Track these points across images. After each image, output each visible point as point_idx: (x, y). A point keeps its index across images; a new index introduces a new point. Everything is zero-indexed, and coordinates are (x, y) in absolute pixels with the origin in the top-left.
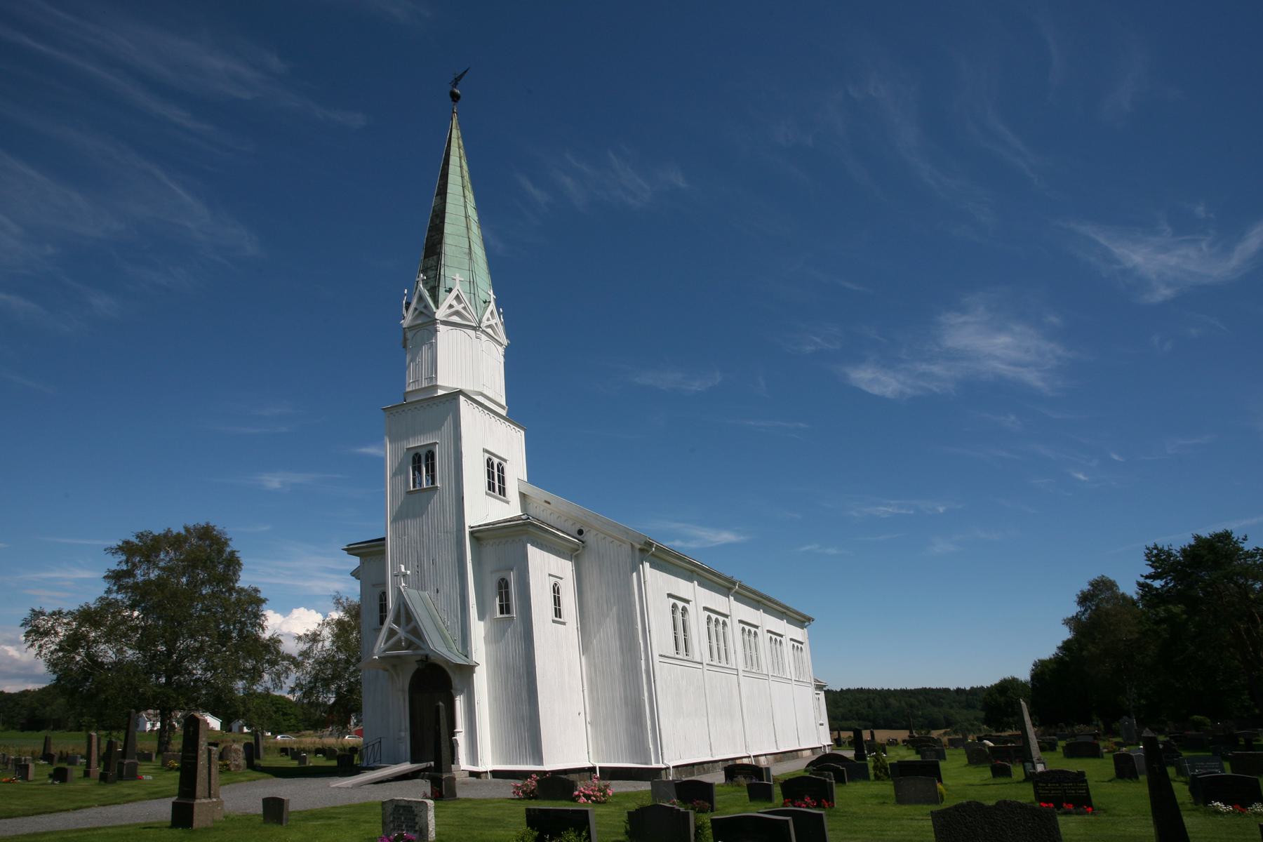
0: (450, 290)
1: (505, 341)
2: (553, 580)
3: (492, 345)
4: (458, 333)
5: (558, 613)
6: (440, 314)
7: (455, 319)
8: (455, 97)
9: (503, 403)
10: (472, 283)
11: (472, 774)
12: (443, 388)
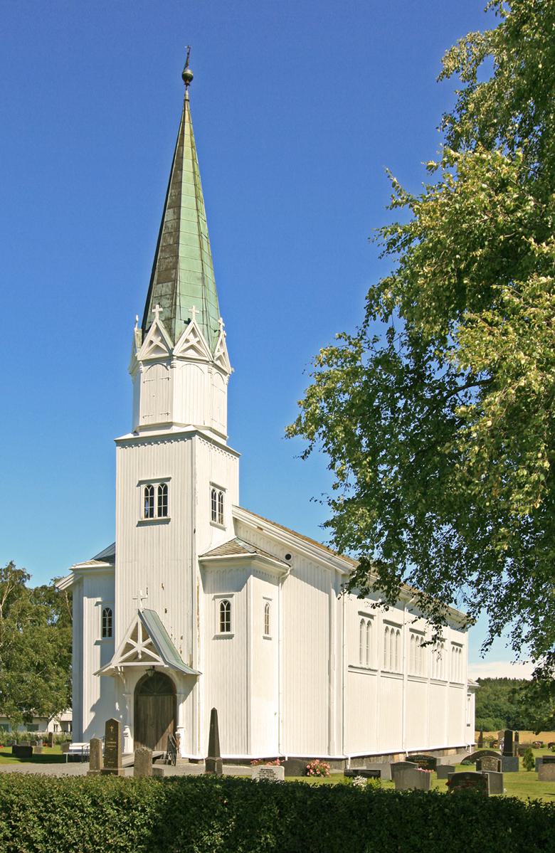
0: (188, 322)
1: (228, 368)
2: (266, 601)
3: (216, 375)
4: (192, 368)
5: (226, 626)
6: (177, 352)
7: (191, 354)
8: (187, 79)
9: (225, 432)
10: (205, 312)
11: (192, 761)
12: (177, 424)
